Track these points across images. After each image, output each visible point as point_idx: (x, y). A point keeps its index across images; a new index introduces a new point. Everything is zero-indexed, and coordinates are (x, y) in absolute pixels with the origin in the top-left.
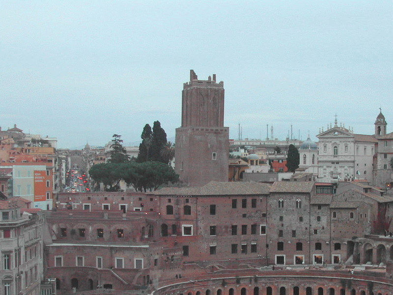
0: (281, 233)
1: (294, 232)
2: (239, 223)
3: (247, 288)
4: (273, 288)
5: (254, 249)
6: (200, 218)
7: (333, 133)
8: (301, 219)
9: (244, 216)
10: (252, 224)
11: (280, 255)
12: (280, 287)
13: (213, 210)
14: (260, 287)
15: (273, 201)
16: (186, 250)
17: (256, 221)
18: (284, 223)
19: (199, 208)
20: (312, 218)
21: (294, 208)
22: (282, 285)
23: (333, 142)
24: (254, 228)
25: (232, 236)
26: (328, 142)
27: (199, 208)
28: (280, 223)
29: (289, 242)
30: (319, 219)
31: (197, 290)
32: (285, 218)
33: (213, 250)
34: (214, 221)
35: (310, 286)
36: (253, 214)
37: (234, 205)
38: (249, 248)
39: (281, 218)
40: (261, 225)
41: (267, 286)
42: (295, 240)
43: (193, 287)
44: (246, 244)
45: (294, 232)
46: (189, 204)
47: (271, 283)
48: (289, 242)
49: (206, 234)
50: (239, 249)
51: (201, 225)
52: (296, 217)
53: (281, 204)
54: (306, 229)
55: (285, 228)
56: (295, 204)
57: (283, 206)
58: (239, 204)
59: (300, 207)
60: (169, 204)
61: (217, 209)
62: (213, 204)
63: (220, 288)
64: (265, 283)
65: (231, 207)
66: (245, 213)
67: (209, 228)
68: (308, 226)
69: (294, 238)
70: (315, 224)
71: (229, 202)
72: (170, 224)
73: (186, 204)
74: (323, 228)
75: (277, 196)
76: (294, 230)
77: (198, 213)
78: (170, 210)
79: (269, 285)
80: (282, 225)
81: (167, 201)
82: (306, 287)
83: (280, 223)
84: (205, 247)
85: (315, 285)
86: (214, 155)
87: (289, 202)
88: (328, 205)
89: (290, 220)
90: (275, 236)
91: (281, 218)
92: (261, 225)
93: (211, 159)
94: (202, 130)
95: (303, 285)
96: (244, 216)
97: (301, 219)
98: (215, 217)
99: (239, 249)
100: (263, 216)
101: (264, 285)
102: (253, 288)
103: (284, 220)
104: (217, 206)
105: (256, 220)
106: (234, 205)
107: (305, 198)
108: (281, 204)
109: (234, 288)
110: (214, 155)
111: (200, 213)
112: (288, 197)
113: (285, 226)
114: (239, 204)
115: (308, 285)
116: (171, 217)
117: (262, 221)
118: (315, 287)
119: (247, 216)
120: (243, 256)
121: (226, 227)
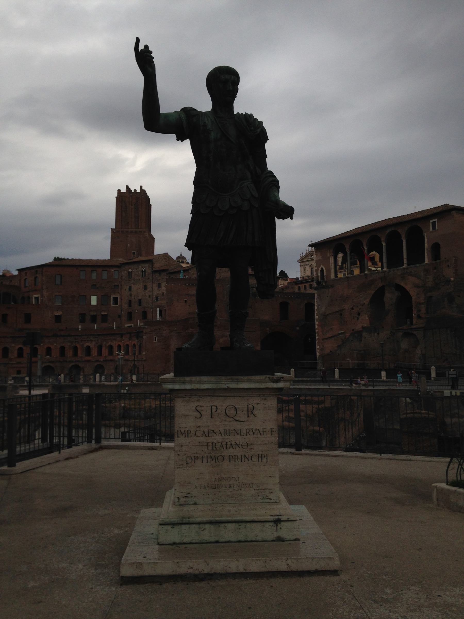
0: (130, 302)
1: (140, 301)
3: (52, 347)
4: (78, 347)
7: (310, 257)
8: (145, 288)
11: (129, 325)
12: (85, 346)
16: (28, 318)
18: (132, 293)
20: (155, 285)
22: (87, 344)
23: (310, 264)
26: (306, 265)
27: (44, 278)
29: (137, 311)
30: (159, 286)
32: (134, 288)
33: (58, 319)
35: (112, 344)
39: (130, 289)
41: (72, 345)
45: (140, 301)
48: (137, 311)
51: (45, 294)
54: (149, 296)
57: (131, 278)
59: (145, 276)
60: (26, 277)
63: (20, 346)
66: (95, 284)
68: (150, 294)
70: (156, 292)
74: (163, 294)
76: (140, 298)
80: (131, 295)
82: (108, 345)
86: (134, 253)
88: (167, 270)
90: (125, 306)
92: (112, 296)
94: (122, 232)
97: (145, 288)
102: (59, 347)
103: (132, 290)
107: (149, 266)
110: (134, 253)
115: (109, 343)
118: (115, 344)
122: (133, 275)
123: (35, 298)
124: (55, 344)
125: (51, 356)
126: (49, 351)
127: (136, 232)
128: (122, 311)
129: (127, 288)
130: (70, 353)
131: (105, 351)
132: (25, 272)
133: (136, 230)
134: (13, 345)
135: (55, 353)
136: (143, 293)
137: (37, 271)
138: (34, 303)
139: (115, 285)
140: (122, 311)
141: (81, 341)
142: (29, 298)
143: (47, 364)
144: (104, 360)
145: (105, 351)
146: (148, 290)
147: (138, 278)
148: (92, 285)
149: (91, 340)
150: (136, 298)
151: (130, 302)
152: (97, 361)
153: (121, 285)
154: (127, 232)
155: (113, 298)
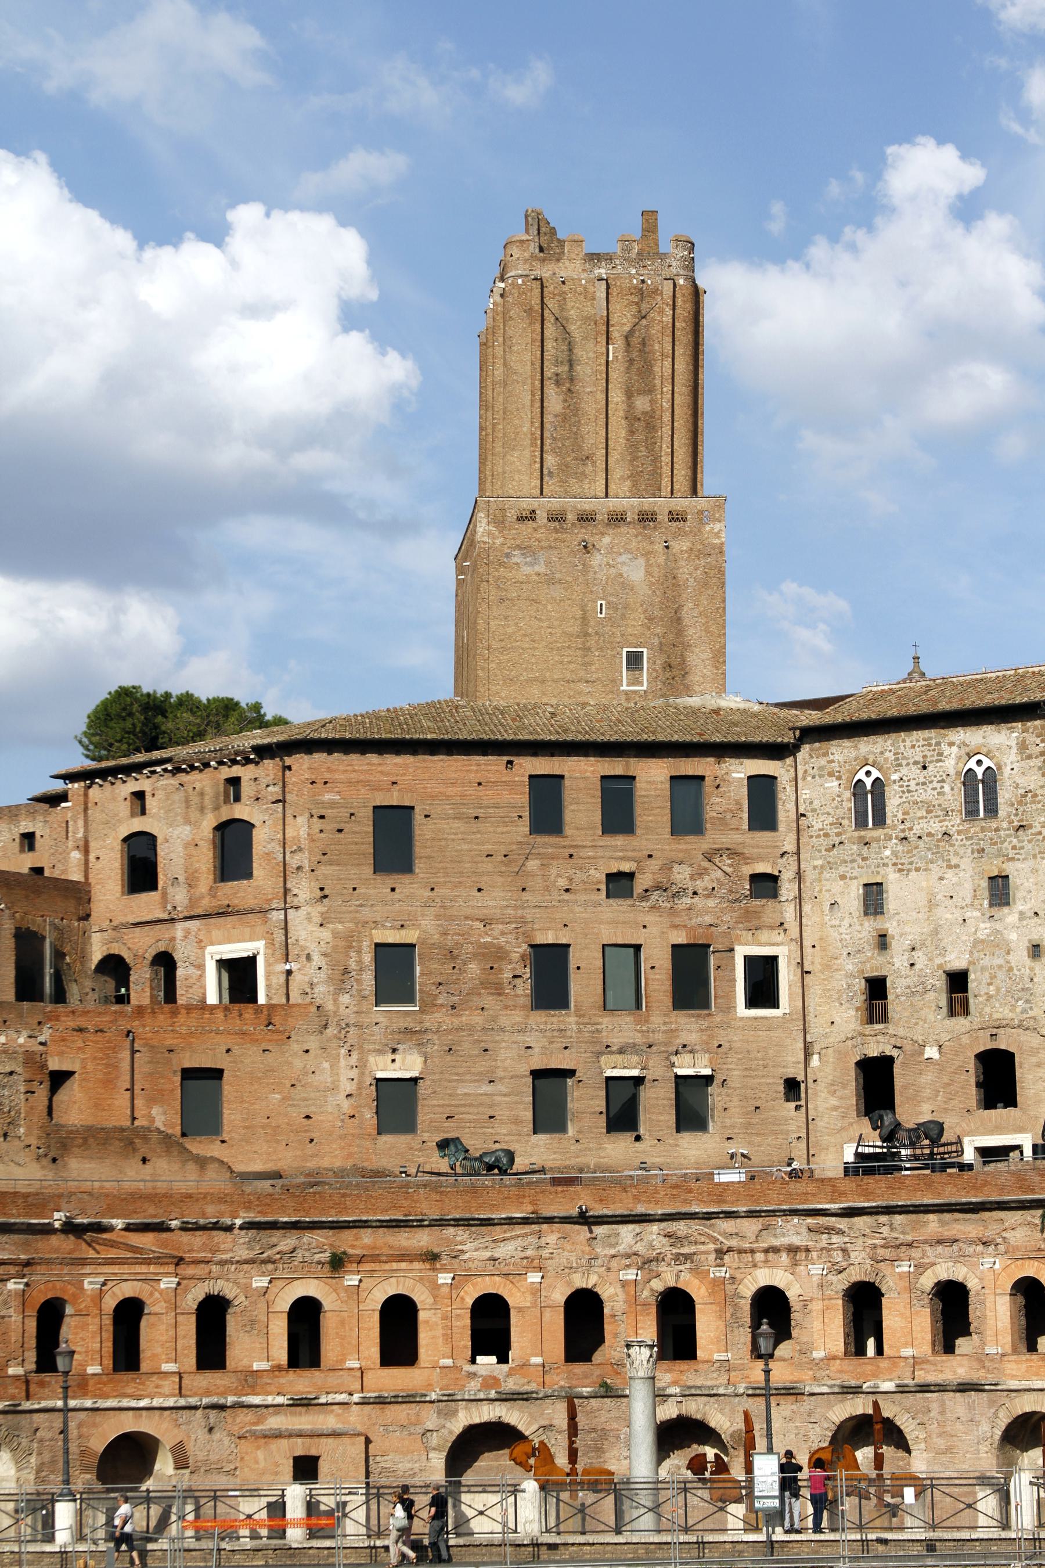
0: (877, 988)
1: (958, 981)
2: (589, 926)
3: (514, 1298)
5: (691, 1105)
6: (303, 889)
8: (999, 891)
9: (619, 883)
10: (681, 939)
12: (748, 1289)
13: (393, 840)
14: (607, 1293)
15: (815, 786)
17: (708, 919)
18: (891, 927)
19: (300, 828)
21: (955, 822)
22: (764, 1277)
24: (691, 976)
25: (539, 1018)
28: (868, 928)
29: (931, 1052)
31: (128, 1290)
32: (898, 892)
33: (396, 1103)
34: (401, 912)
35: (959, 1273)
36: (681, 875)
37: (546, 807)
38: (657, 1106)
39: (874, 898)
40: (742, 951)
41: (658, 1285)
42: (968, 1036)
43: (83, 1262)
44: (635, 1073)
46: (241, 811)
47: (688, 1257)
48: (931, 1052)
49: (345, 999)
50: (586, 1102)
51: (307, 930)
52: (967, 879)
53: (870, 804)
55: (896, 968)
56: (954, 796)
57: (880, 820)
58: (582, 808)
59: (992, 810)
60: (138, 825)
61: (423, 831)
62: (394, 799)
64: (648, 1263)
65: (524, 826)
66: (626, 867)
67: (368, 958)
69: (961, 1023)
71: (509, 782)
72: (137, 948)
73: (227, 813)
75: (841, 751)
76: (958, 964)
77: (293, 861)
78: (142, 869)
79: (668, 1277)
80: (883, 941)
81: (124, 808)
82: (927, 1281)
83: (868, 928)
84: (335, 1081)
85: (988, 1261)
86: (634, 660)
87: (923, 771)
89: (932, 904)
90: (838, 1020)
91: (874, 898)
92: (742, 951)
93: (616, 682)
94: (557, 517)
95: (904, 1267)
96: (619, 883)
97: (999, 891)
98: (410, 887)
99: (586, 1102)
100: (755, 894)
101: (630, 1275)
102: (559, 1296)
104: (418, 815)
105: (705, 912)
106: (546, 807)
107: (1023, 746)
108: (870, 804)
109: (420, 1296)
110: (634, 660)
111: (303, 859)
112: (913, 744)
113: (898, 946)
114: (582, 808)
115: (945, 1271)
116: (146, 905)
117: (752, 923)
119: (638, 890)
120: (618, 1149)
121: (494, 956)
122: (893, 804)
123: (224, 964)
124: (534, 1278)
125: (503, 1359)
126: (490, 1326)
127: (647, 518)
128: (808, 1054)
129: (853, 897)
130: (631, 1335)
131: (908, 1323)
132: (132, 785)
133: (648, 503)
134: (260, 1282)
135: (537, 1333)
136: (985, 929)
137: (234, 782)
138: (212, 999)
139: (755, 878)
140: (808, 1054)
141: (720, 1253)
142: (165, 962)
143: (487, 1413)
144: (902, 1390)
145: (908, 1323)
146: (1019, 906)
147: (936, 827)
148: (609, 876)
149: (793, 1250)
150: (920, 957)
151: (877, 988)
152: (855, 1391)
153: (799, 875)
154: (586, 518)
155: (749, 960)
